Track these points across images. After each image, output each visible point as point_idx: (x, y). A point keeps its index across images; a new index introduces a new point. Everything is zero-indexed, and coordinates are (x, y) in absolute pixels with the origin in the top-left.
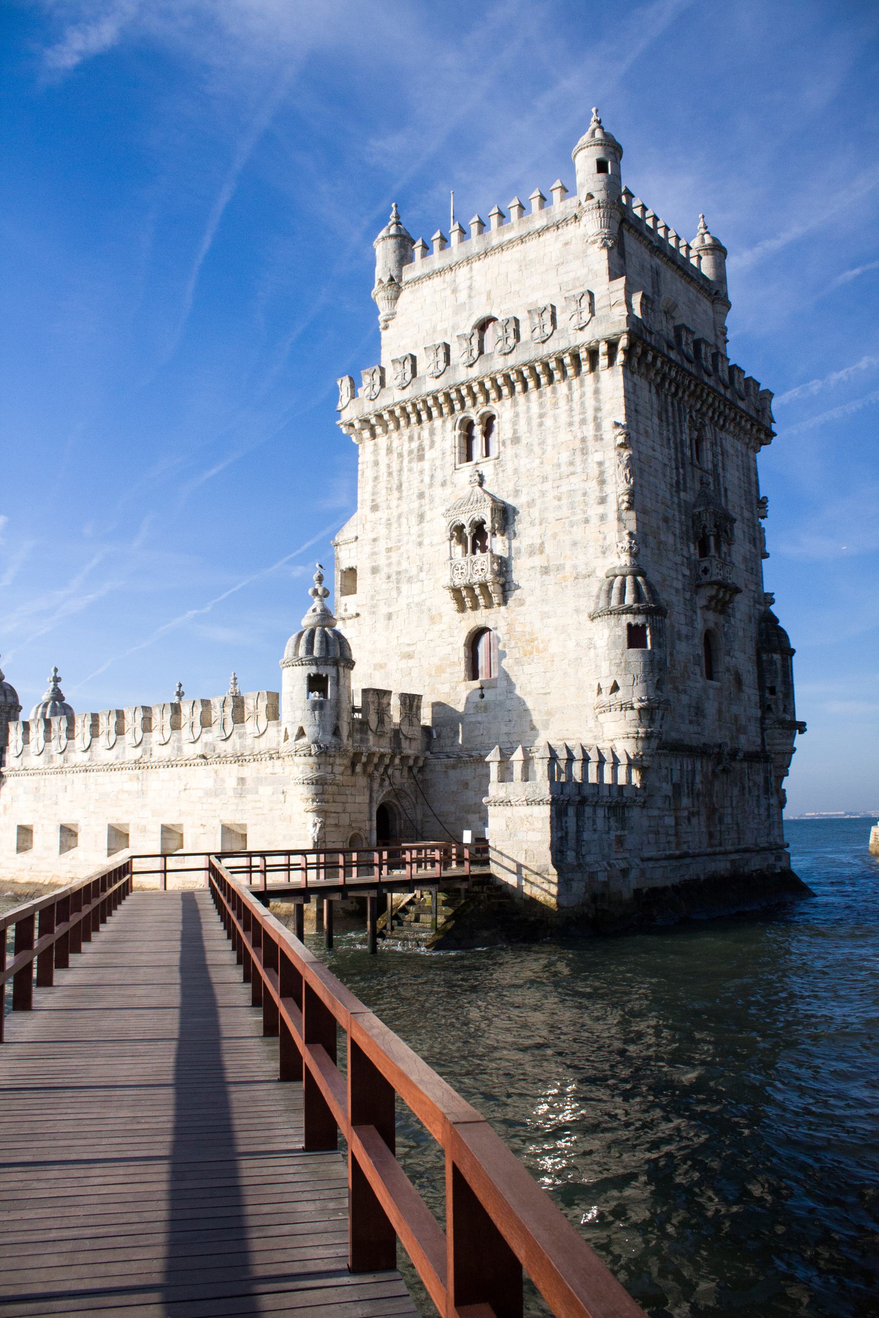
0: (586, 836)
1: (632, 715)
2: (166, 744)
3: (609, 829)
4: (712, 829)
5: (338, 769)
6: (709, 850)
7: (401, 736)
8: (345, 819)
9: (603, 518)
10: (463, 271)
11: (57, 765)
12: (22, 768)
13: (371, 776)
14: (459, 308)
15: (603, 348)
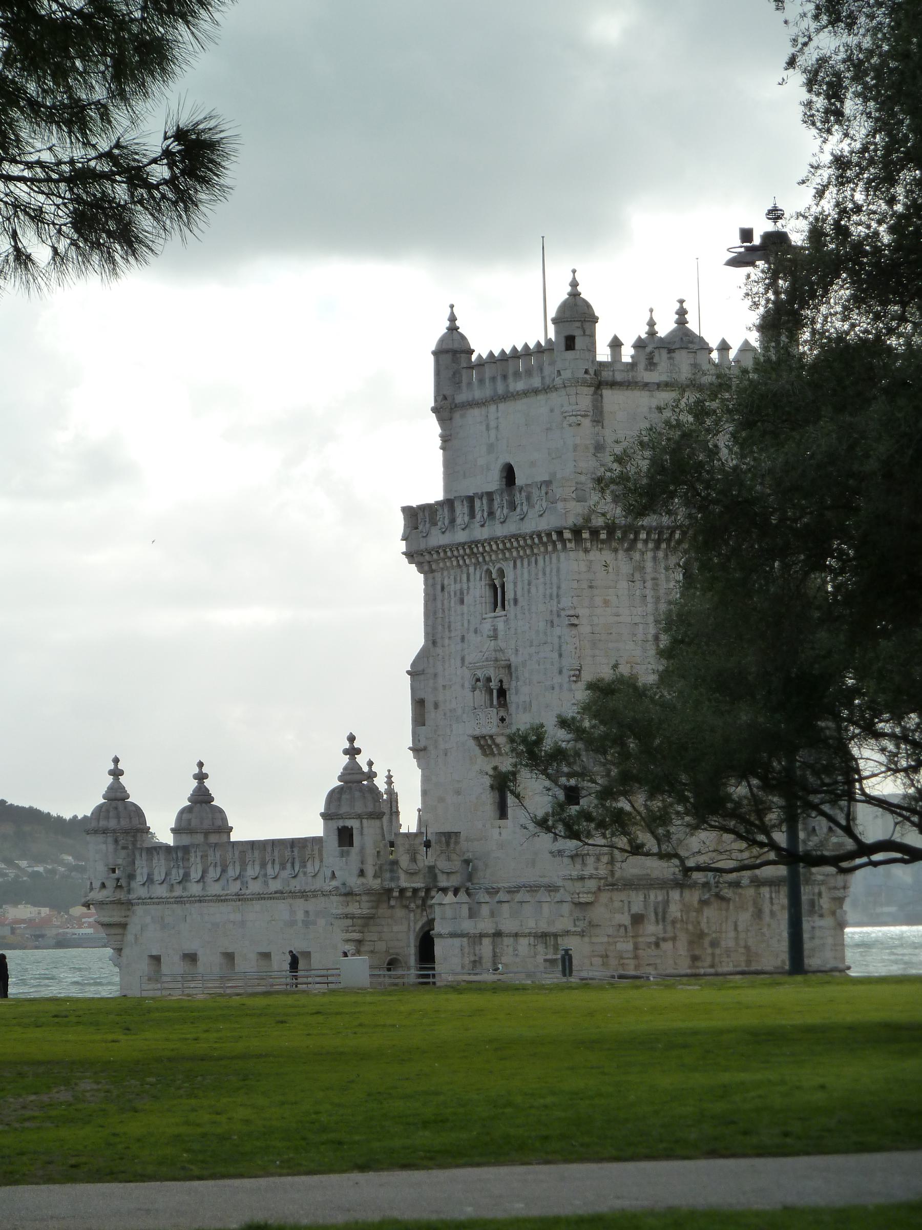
0: (504, 959)
1: (566, 860)
2: (256, 878)
3: (535, 954)
4: (697, 953)
5: (365, 905)
6: (689, 971)
7: (437, 871)
8: (381, 946)
9: (561, 687)
10: (493, 408)
11: (176, 894)
12: (148, 896)
13: (407, 907)
14: (491, 448)
15: (554, 537)
